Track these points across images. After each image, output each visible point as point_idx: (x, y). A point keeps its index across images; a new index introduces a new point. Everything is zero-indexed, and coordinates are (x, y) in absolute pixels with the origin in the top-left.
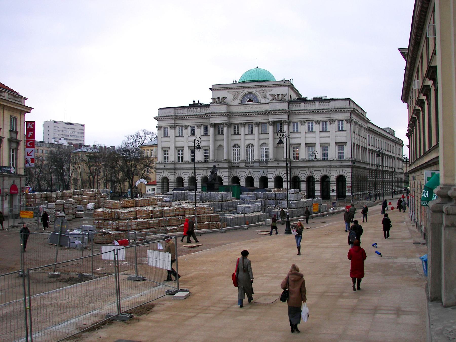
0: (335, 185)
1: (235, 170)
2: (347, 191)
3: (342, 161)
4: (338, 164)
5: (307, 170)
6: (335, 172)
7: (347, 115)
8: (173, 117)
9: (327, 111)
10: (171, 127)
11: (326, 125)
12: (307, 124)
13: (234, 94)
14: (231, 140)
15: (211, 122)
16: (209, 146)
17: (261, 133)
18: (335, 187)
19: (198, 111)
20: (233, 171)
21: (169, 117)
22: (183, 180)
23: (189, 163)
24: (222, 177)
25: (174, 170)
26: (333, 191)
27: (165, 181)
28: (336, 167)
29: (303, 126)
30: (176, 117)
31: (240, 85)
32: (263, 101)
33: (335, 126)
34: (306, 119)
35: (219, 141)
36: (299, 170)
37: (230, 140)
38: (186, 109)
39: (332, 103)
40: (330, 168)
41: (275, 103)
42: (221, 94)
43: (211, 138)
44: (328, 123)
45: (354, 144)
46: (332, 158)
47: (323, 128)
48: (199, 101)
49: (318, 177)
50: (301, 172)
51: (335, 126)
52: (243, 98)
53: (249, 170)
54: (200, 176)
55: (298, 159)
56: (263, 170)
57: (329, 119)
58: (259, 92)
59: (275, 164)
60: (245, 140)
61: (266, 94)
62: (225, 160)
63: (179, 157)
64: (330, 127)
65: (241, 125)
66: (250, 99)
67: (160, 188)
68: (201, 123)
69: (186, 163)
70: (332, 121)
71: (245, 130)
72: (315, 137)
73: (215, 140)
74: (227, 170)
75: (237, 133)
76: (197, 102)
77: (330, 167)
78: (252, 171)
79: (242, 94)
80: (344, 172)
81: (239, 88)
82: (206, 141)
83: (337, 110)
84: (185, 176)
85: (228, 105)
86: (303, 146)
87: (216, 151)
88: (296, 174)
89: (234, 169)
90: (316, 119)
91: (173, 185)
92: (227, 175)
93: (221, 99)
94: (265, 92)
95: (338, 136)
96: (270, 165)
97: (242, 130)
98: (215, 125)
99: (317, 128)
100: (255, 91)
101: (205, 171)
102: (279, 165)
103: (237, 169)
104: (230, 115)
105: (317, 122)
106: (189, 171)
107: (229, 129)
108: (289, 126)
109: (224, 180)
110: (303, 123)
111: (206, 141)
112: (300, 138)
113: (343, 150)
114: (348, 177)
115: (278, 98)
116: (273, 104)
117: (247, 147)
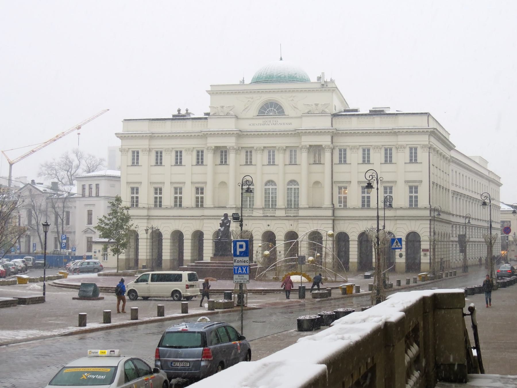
2: (422, 257)
7: (424, 140)
9: (395, 133)
10: (143, 150)
16: (205, 183)
17: (288, 163)
19: (188, 127)
23: (171, 208)
25: (148, 219)
26: (401, 256)
38: (169, 123)
39: (401, 118)
42: (227, 101)
45: (433, 183)
48: (187, 110)
51: (405, 155)
56: (291, 222)
63: (156, 198)
66: (272, 109)
75: (249, 163)
76: (183, 112)
78: (274, 222)
96: (302, 213)
101: (198, 222)
104: (240, 134)
110: (354, 148)
117: (266, 185)
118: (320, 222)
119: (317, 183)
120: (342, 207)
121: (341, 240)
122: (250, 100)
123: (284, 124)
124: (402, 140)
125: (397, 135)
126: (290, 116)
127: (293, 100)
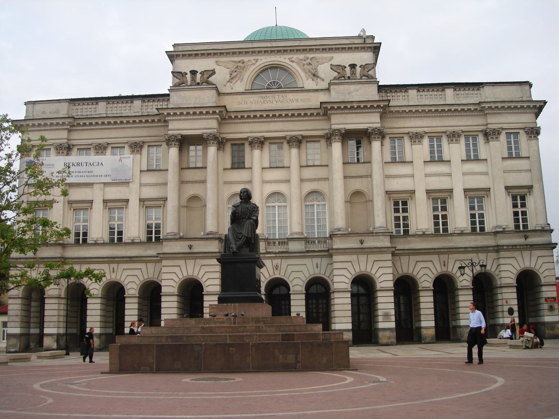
0: (515, 295)
2: (546, 312)
3: (528, 234)
4: (518, 240)
5: (435, 258)
6: (513, 261)
8: (67, 121)
9: (481, 109)
11: (475, 145)
12: (426, 141)
13: (232, 66)
14: (226, 183)
15: (170, 133)
16: (165, 199)
18: (515, 302)
21: (55, 122)
23: (104, 244)
24: (202, 281)
26: (511, 312)
27: (34, 296)
28: (513, 248)
29: (416, 147)
30: (73, 124)
31: (250, 45)
33: (499, 146)
34: (427, 130)
35: (190, 185)
36: (413, 258)
37: (221, 182)
39: (486, 88)
40: (497, 251)
41: (346, 86)
42: (201, 65)
43: (172, 176)
44: (481, 139)
47: (468, 151)
50: (421, 265)
53: (277, 262)
55: (406, 232)
56: (316, 260)
59: (353, 243)
60: (264, 182)
61: (316, 69)
62: (211, 233)
64: (484, 149)
65: (251, 143)
67: (19, 313)
68: (142, 139)
70: (490, 135)
71: (261, 157)
72: (450, 175)
73: (182, 182)
75: (238, 164)
77: (498, 249)
79: (253, 67)
81: (247, 52)
83: (506, 105)
85: (219, 94)
86: (421, 195)
87: (184, 211)
88: (405, 271)
90: (451, 129)
91: (56, 306)
93: (198, 76)
94: (314, 63)
95: (510, 171)
96: (338, 244)
97: (256, 158)
98: (184, 142)
99: (455, 151)
100: (287, 61)
102: (365, 245)
104: (224, 116)
105: (453, 136)
107: (221, 153)
108: (382, 145)
109: (206, 290)
110: (416, 137)
112: (412, 176)
113: (523, 205)
115: (353, 73)
116: (342, 87)
118: (372, 257)
119: (357, 193)
120: (402, 233)
121: (405, 288)
122: (240, 64)
124: (495, 121)
125: (486, 115)
126: (307, 87)
127: (310, 64)
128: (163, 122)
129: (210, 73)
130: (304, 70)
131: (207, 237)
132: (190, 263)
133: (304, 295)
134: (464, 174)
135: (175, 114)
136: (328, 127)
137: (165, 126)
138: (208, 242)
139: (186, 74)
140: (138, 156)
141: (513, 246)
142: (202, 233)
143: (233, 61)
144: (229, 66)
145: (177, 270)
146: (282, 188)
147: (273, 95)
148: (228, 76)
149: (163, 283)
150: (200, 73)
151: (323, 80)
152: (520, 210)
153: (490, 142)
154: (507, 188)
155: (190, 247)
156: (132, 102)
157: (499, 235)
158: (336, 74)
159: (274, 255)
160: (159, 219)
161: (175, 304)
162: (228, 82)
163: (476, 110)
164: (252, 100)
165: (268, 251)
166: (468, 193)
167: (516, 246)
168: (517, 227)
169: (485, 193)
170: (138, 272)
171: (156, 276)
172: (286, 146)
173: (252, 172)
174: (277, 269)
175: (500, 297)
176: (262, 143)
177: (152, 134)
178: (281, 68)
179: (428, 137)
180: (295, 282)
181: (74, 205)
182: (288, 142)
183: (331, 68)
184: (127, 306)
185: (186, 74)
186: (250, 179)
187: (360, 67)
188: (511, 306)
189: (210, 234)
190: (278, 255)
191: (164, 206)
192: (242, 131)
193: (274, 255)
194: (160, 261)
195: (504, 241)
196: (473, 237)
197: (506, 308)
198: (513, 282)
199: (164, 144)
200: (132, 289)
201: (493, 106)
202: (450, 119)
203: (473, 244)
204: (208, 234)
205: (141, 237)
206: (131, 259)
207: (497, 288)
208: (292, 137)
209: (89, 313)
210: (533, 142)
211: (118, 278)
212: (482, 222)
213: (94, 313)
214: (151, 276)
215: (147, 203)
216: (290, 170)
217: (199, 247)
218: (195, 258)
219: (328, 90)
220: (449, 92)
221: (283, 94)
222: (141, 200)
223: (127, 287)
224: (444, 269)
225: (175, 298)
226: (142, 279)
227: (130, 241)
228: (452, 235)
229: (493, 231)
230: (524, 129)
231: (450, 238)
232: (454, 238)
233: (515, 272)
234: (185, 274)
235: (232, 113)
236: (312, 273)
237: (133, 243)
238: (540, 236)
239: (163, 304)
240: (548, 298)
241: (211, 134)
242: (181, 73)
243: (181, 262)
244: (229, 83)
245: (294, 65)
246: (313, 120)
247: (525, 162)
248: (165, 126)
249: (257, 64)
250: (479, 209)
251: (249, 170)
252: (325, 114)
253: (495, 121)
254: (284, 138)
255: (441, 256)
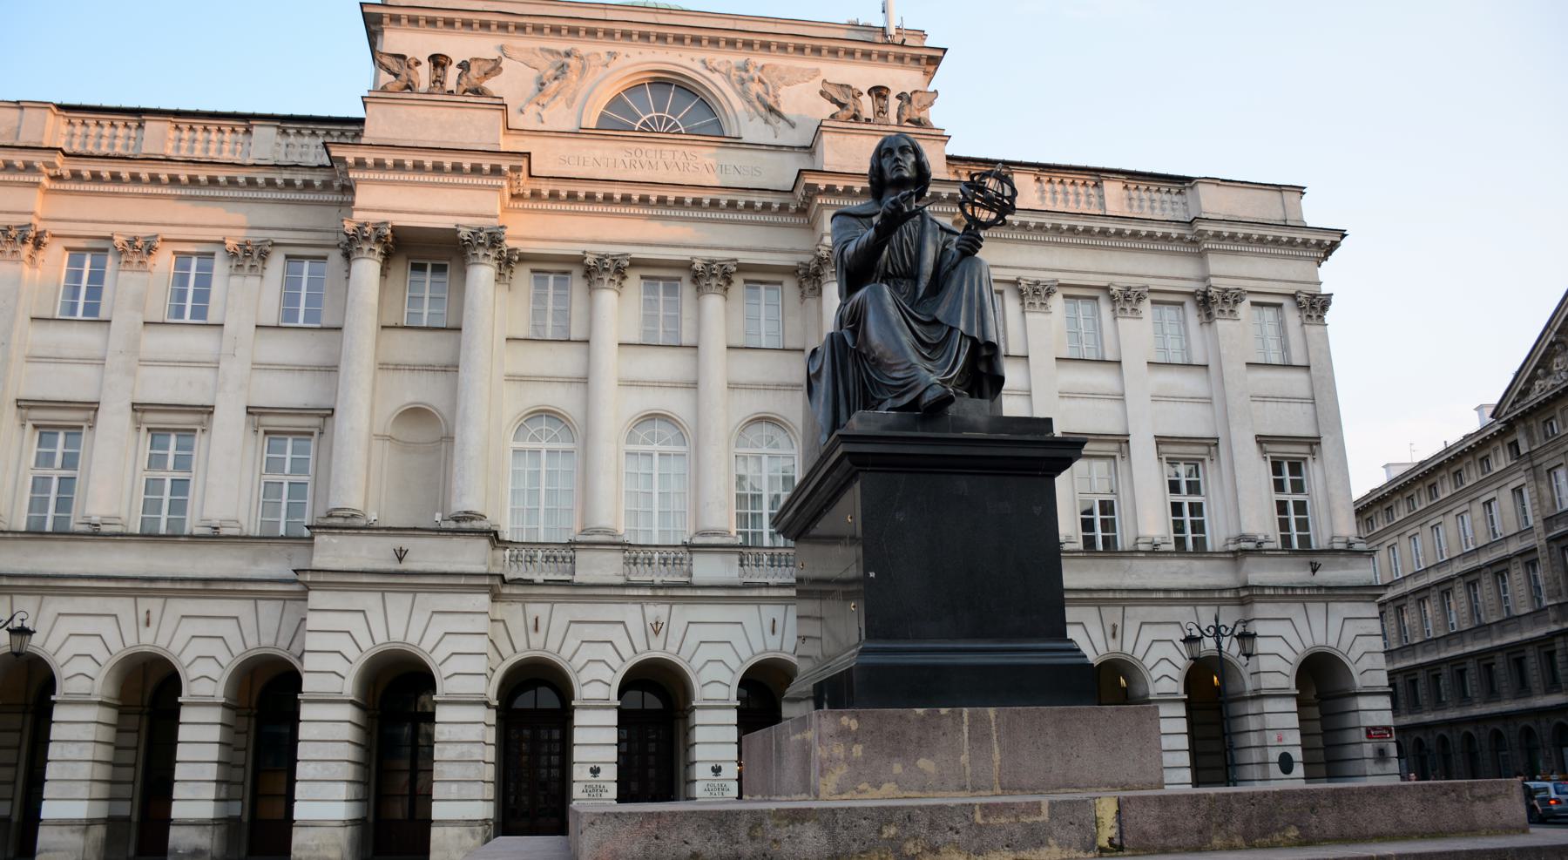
0: (1293, 721)
1: (538, 610)
3: (1318, 559)
4: (1292, 573)
9: (1193, 238)
14: (511, 378)
15: (359, 216)
18: (1295, 738)
20: (512, 614)
22: (49, 683)
24: (434, 661)
26: (1286, 763)
28: (1288, 594)
32: (754, 129)
34: (1064, 278)
46: (1242, 538)
49: (1165, 668)
52: (616, 103)
53: (656, 611)
54: (216, 648)
56: (771, 612)
57: (1201, 286)
58: (728, 76)
62: (469, 516)
69: (95, 534)
74: (482, 601)
77: (1246, 596)
78: (682, 615)
80: (1335, 623)
82: (302, 369)
83: (1256, 232)
84: (75, 646)
89: (524, 600)
90: (1119, 283)
92: (481, 644)
93: (453, 73)
100: (699, 67)
101: (269, 609)
103: (552, 600)
105: (1125, 299)
106: (122, 606)
111: (302, 369)
113: (1298, 487)
114: (1367, 662)
123: (723, 169)
124: (1226, 270)
125: (1201, 255)
128: (337, 192)
129: (488, 67)
130: (744, 94)
131: (452, 525)
132: (399, 603)
133: (734, 713)
134: (1156, 399)
135: (379, 165)
136: (808, 246)
137: (341, 204)
138: (457, 542)
139: (418, 63)
140: (253, 281)
141: (1286, 588)
142: (438, 517)
143: (551, 52)
144: (537, 61)
145: (354, 623)
146: (675, 403)
147: (659, 147)
148: (534, 86)
149: (310, 663)
150: (460, 66)
151: (793, 125)
152: (1290, 498)
153: (1218, 322)
154: (1262, 440)
155: (401, 555)
156: (248, 132)
157: (1250, 560)
158: (835, 108)
159: (649, 592)
160: (305, 472)
161: (348, 732)
162: (530, 102)
163: (1181, 238)
164: (598, 154)
165: (633, 578)
166: (1163, 448)
167: (1293, 588)
168: (1286, 540)
169: (1204, 449)
170: (227, 629)
171: (283, 643)
172: (687, 289)
173: (588, 354)
174: (657, 633)
175: (1253, 723)
176: (621, 272)
177: (298, 224)
178: (682, 87)
179: (1065, 296)
180: (706, 676)
181: (35, 414)
182: (696, 278)
183: (822, 93)
184: (184, 733)
185: (418, 63)
186: (580, 373)
187: (899, 97)
188: (1286, 750)
189: (464, 519)
190: (661, 592)
191: (321, 433)
192: (565, 234)
193: (649, 592)
194: (303, 596)
195: (1260, 573)
196: (1181, 563)
197: (1274, 755)
198: (1289, 683)
199: (335, 256)
200: (206, 680)
201: (1226, 230)
202: (1117, 255)
203: (1184, 581)
204: (457, 520)
205: (244, 522)
206: (207, 587)
207: (1245, 699)
208: (709, 263)
209: (54, 751)
210: (1313, 330)
211: (162, 642)
212: (1198, 527)
213: (72, 752)
214: (268, 641)
215: (272, 422)
216: (697, 356)
217: (428, 555)
218: (415, 589)
219: (809, 150)
220: (1112, 189)
221: (687, 149)
222: (250, 411)
223: (186, 676)
224: (1114, 646)
225: (348, 712)
226: (238, 649)
227: (207, 531)
228: (1133, 553)
229: (1231, 547)
230: (1294, 296)
231: (1126, 562)
232: (1136, 562)
233: (1291, 656)
234: (381, 638)
235: (543, 182)
236: (758, 647)
237: (214, 537)
238: (1345, 566)
239: (304, 731)
240: (1374, 728)
241: (481, 230)
242: (403, 57)
243: (370, 601)
244: (534, 108)
245: (716, 78)
246: (768, 224)
247: (1299, 377)
248: (341, 204)
249: (615, 65)
250: (1190, 492)
251: (582, 346)
252: (802, 211)
253: (1226, 270)
254: (687, 266)
255: (1106, 611)
